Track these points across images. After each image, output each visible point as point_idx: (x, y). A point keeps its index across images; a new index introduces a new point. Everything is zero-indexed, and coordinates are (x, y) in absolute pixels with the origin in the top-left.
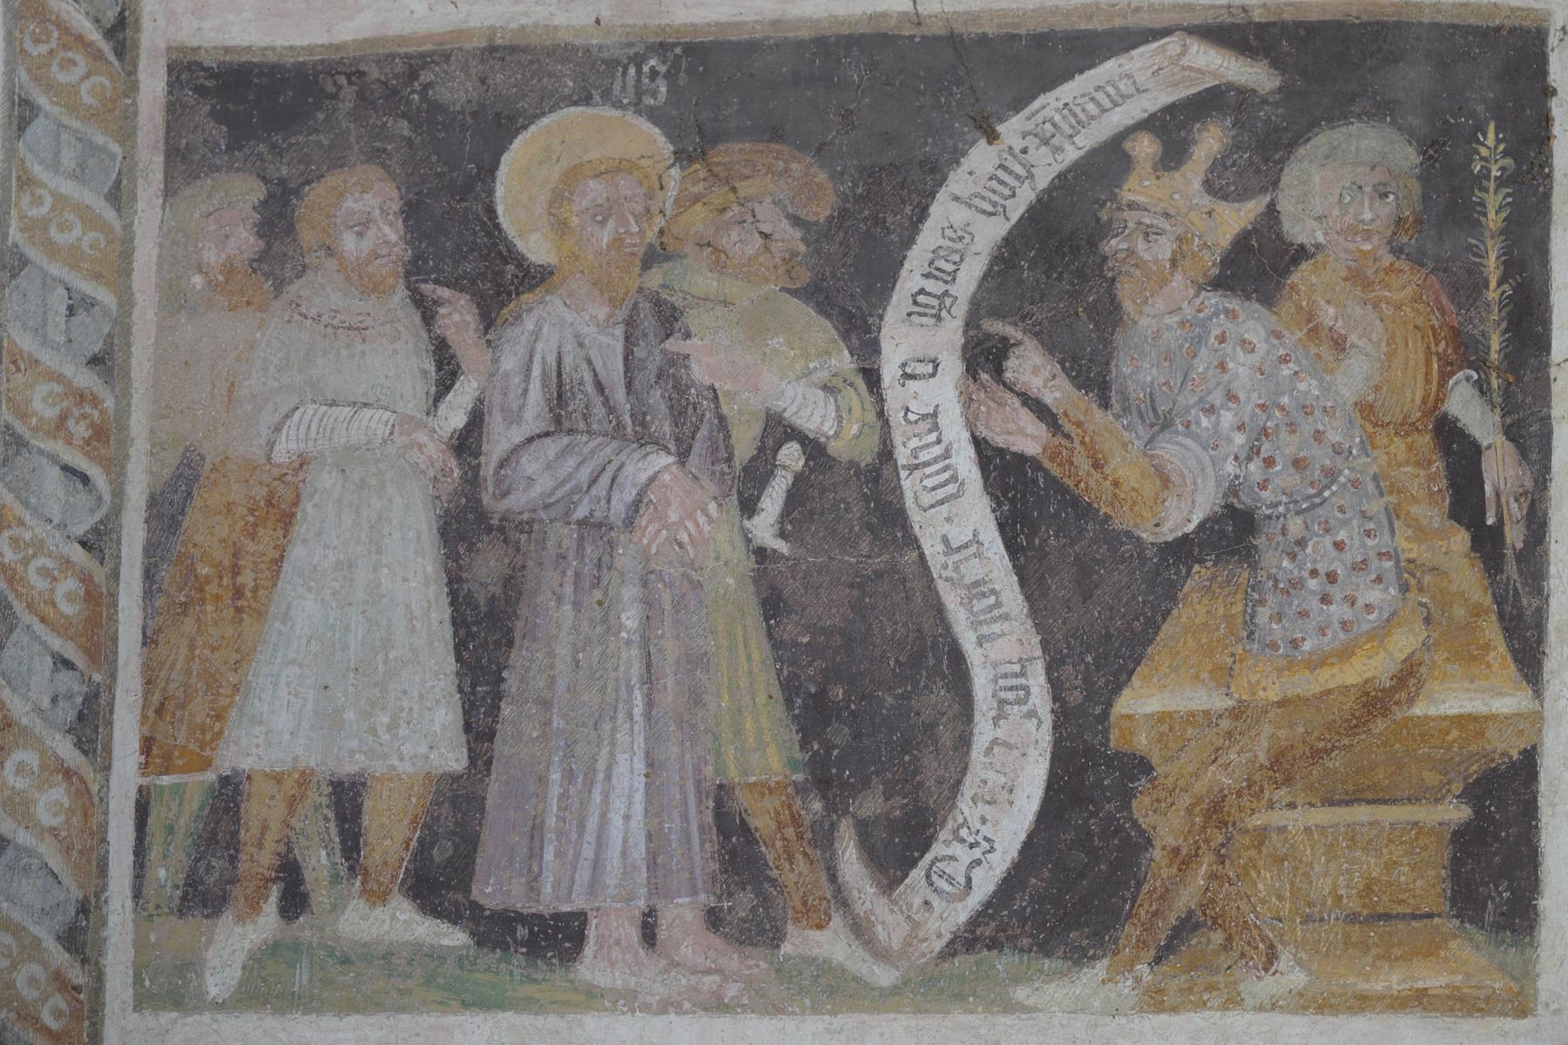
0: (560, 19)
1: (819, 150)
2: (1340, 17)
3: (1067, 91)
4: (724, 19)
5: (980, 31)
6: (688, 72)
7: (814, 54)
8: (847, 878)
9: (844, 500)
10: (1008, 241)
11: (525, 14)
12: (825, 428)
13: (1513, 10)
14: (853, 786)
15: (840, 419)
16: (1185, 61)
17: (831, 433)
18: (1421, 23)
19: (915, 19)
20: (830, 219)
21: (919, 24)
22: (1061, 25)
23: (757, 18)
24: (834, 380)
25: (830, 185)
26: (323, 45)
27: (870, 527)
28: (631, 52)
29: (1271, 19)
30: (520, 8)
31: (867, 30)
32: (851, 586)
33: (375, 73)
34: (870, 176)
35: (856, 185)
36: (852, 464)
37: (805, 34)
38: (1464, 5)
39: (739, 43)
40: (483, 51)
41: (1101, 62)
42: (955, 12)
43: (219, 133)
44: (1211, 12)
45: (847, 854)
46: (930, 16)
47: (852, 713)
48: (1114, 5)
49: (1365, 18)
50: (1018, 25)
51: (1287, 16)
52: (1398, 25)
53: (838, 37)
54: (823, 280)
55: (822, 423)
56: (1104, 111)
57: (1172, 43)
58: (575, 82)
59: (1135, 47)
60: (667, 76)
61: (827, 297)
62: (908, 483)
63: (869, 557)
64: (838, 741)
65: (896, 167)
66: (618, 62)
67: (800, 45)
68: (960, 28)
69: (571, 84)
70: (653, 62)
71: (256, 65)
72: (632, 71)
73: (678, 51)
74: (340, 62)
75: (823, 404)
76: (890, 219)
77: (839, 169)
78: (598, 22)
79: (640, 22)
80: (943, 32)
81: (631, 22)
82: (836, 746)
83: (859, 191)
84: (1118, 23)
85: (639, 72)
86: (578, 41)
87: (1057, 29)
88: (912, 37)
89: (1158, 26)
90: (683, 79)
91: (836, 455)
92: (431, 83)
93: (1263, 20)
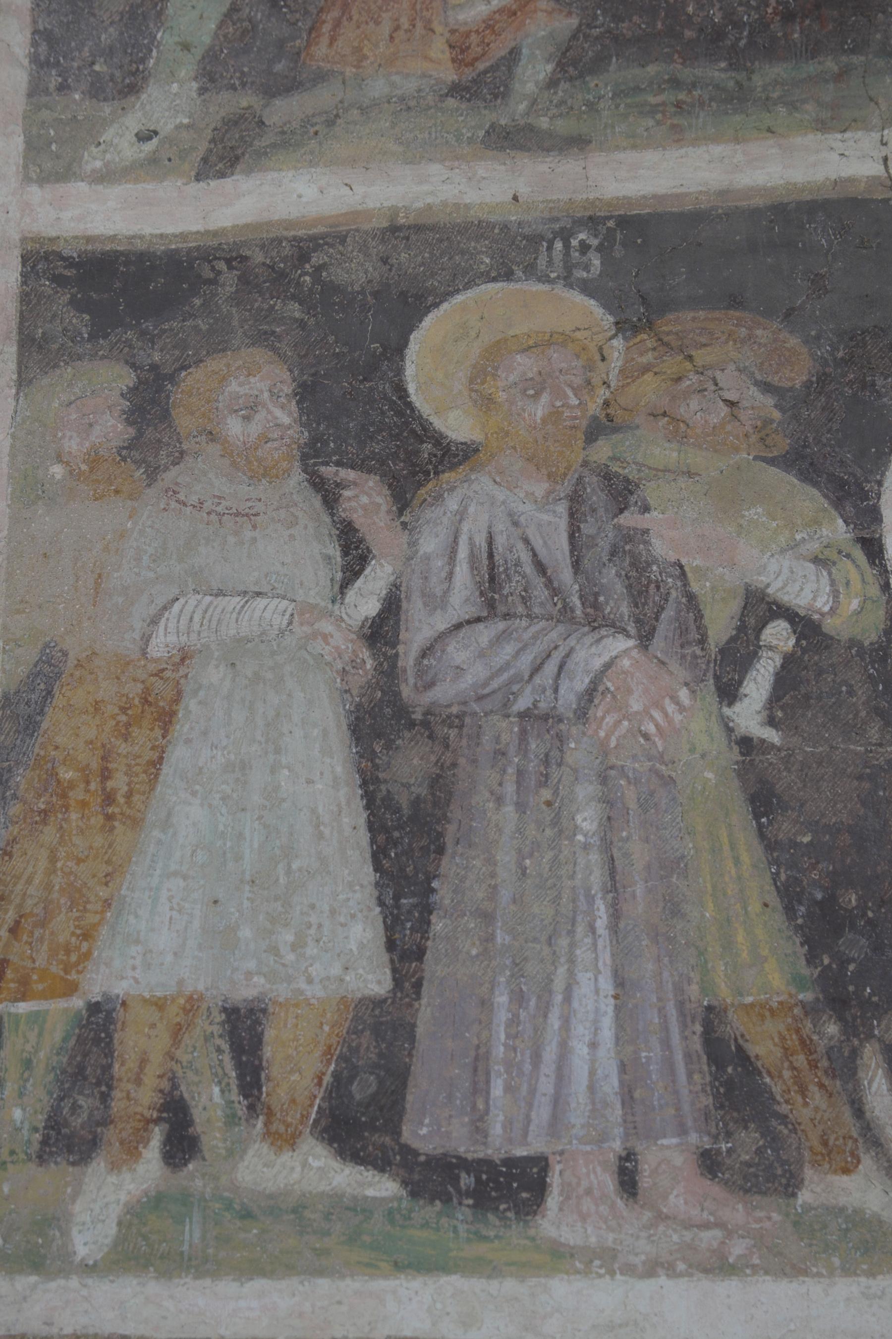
0: (471, 197)
1: (787, 315)
4: (661, 191)
6: (624, 244)
7: (771, 221)
9: (845, 682)
11: (432, 193)
12: (818, 604)
15: (835, 594)
17: (826, 609)
20: (807, 385)
23: (700, 188)
24: (827, 552)
25: (805, 350)
26: (198, 232)
27: (879, 712)
28: (557, 226)
30: (426, 188)
31: (833, 196)
32: (860, 778)
33: (259, 257)
34: (851, 339)
35: (835, 349)
36: (853, 642)
39: (681, 215)
40: (384, 231)
43: (81, 322)
47: (869, 922)
54: (805, 447)
55: (814, 599)
58: (492, 258)
60: (600, 249)
61: (811, 464)
63: (881, 745)
64: (854, 954)
65: (882, 329)
66: (542, 238)
67: (754, 213)
69: (487, 261)
70: (582, 236)
71: (122, 253)
72: (559, 245)
73: (611, 224)
74: (219, 247)
75: (814, 578)
76: (880, 382)
77: (813, 333)
78: (515, 198)
79: (565, 197)
81: (555, 197)
82: (853, 960)
83: (840, 354)
85: (567, 246)
86: (493, 218)
90: (618, 252)
91: (833, 633)
92: (325, 264)
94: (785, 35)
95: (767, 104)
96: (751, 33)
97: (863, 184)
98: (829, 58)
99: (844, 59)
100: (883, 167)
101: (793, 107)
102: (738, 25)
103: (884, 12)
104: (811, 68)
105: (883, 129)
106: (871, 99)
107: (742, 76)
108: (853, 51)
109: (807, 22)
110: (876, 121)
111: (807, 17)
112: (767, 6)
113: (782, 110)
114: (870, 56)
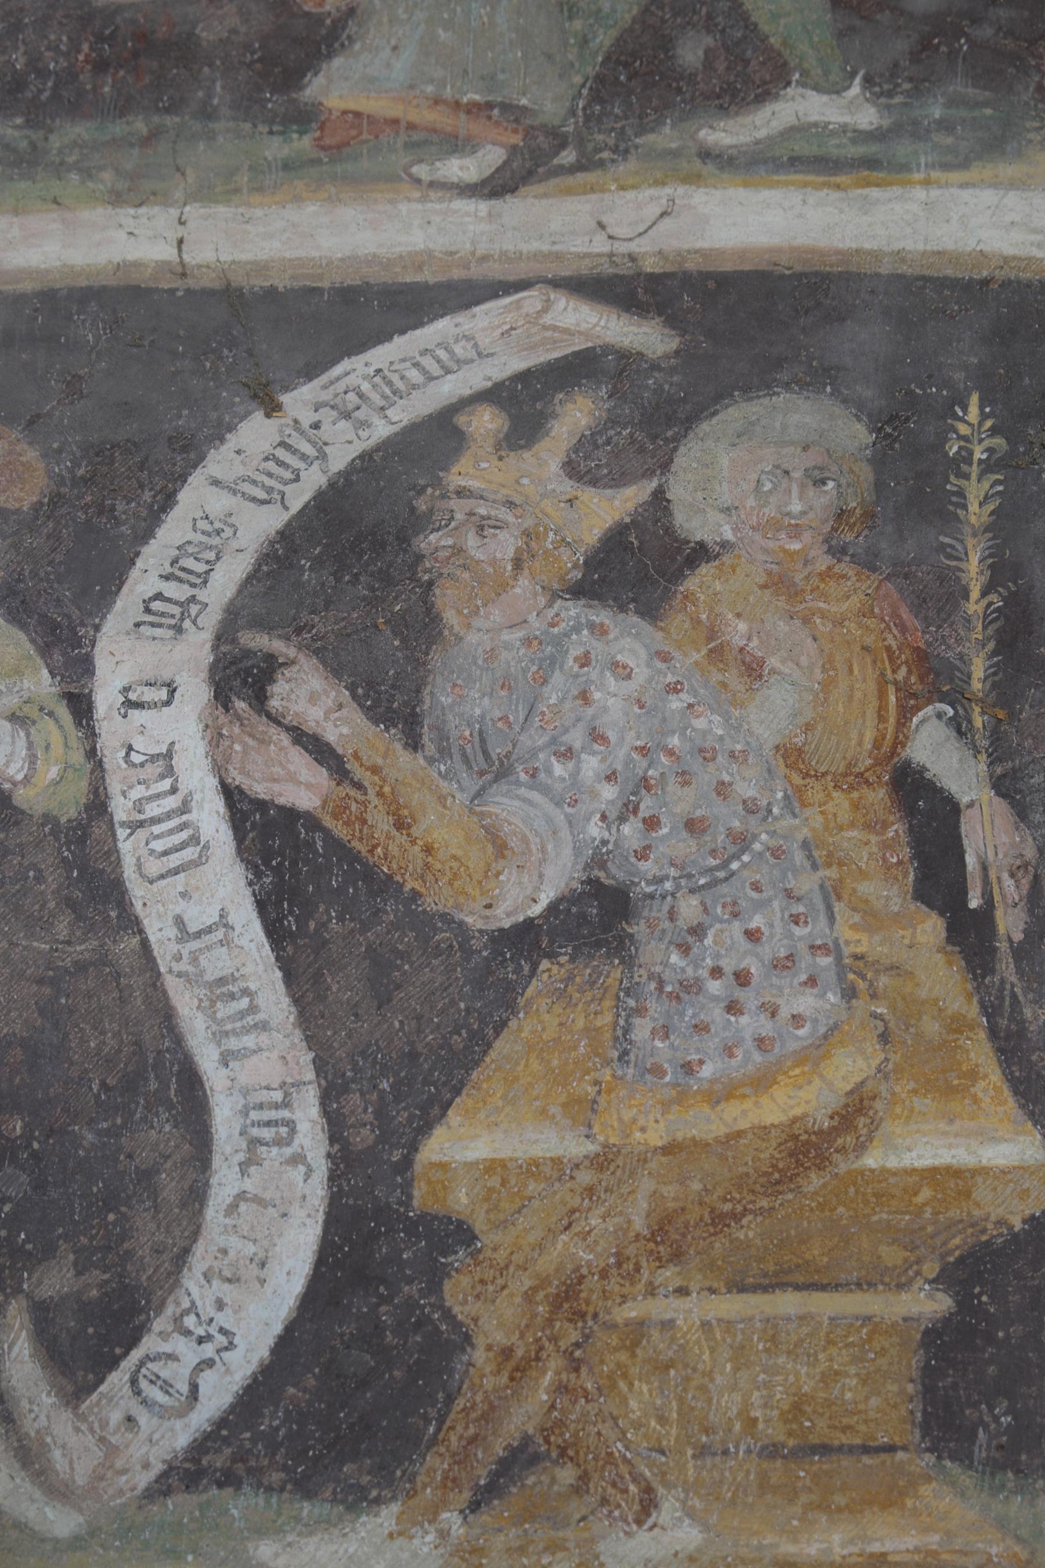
1: (31, 423)
2: (764, 267)
3: (380, 355)
5: (267, 284)
7: (36, 310)
8: (14, 1382)
9: (34, 866)
10: (284, 535)
12: (11, 771)
13: (1006, 260)
14: (30, 1254)
15: (32, 759)
16: (547, 319)
17: (20, 777)
18: (878, 275)
19: (180, 270)
20: (37, 507)
21: (184, 275)
22: (377, 276)
24: (26, 709)
25: (42, 465)
27: (71, 904)
29: (669, 268)
31: (113, 282)
32: (40, 981)
34: (97, 455)
35: (76, 464)
36: (47, 818)
37: (28, 286)
38: (939, 253)
41: (431, 321)
42: (233, 262)
44: (587, 261)
45: (16, 1349)
46: (200, 266)
47: (35, 1155)
48: (452, 253)
49: (798, 268)
50: (321, 277)
51: (690, 266)
52: (847, 277)
53: (71, 290)
54: (19, 581)
55: (7, 764)
56: (432, 378)
57: (531, 299)
59: (477, 303)
61: (23, 602)
62: (127, 846)
63: (69, 943)
64: (12, 1192)
65: (135, 444)
67: (19, 299)
68: (238, 280)
75: (8, 739)
76: (121, 506)
77: (55, 445)
80: (217, 285)
82: (9, 1199)
83: (81, 472)
84: (457, 274)
87: (372, 281)
88: (172, 291)
89: (511, 278)
91: (24, 806)
93: (657, 270)
94: (95, 89)
95: (59, 170)
96: (56, 86)
97: (149, 271)
98: (140, 117)
99: (156, 119)
100: (176, 251)
101: (88, 174)
102: (43, 74)
103: (210, 66)
104: (117, 129)
105: (185, 205)
106: (178, 170)
107: (37, 135)
108: (168, 111)
109: (122, 73)
110: (179, 195)
111: (122, 67)
112: (79, 51)
113: (74, 177)
114: (187, 118)
